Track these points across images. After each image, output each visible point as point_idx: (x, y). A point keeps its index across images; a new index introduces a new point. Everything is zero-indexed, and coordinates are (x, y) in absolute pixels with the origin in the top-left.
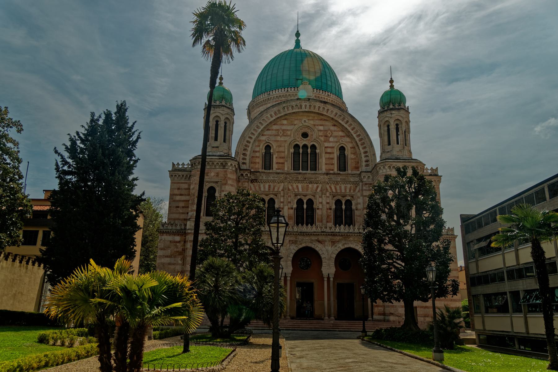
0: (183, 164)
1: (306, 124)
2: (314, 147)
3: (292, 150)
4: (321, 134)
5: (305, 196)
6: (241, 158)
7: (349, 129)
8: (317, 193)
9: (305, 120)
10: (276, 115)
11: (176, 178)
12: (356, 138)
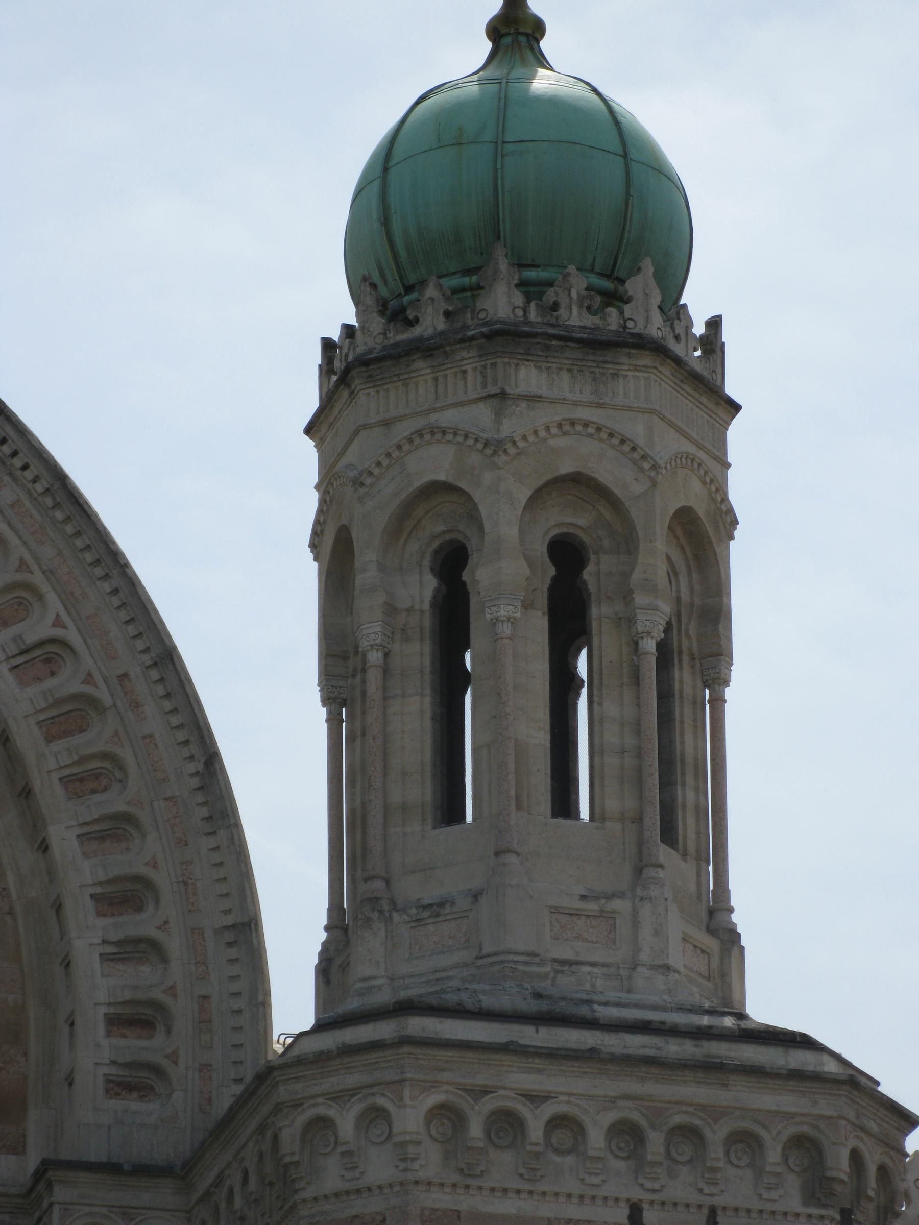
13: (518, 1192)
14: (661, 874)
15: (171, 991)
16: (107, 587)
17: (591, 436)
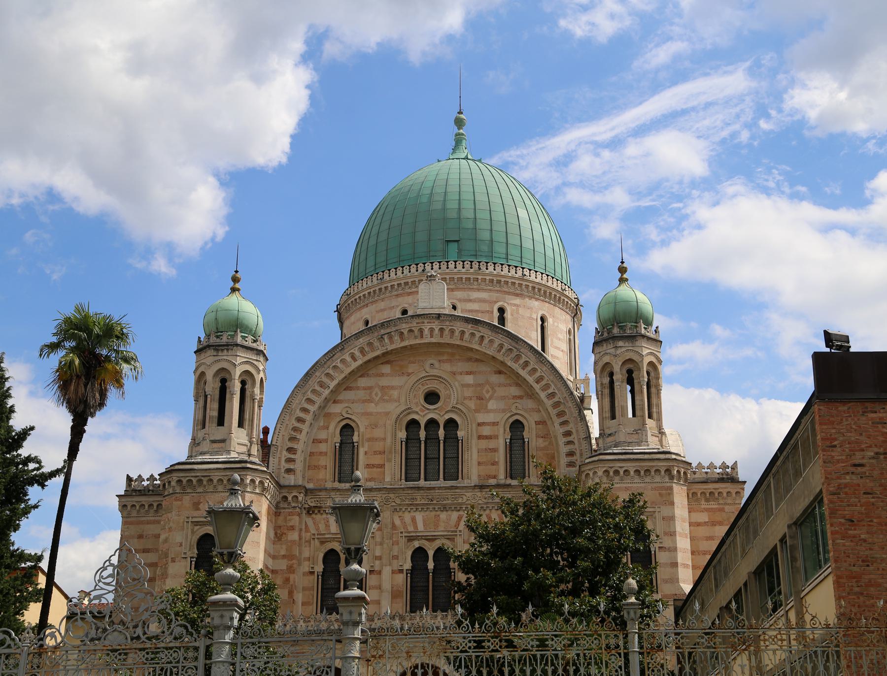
0: (152, 478)
2: (451, 424)
3: (402, 435)
4: (468, 393)
5: (431, 539)
6: (283, 459)
7: (530, 380)
8: (458, 533)
9: (432, 361)
10: (364, 355)
11: (134, 513)
12: (545, 400)
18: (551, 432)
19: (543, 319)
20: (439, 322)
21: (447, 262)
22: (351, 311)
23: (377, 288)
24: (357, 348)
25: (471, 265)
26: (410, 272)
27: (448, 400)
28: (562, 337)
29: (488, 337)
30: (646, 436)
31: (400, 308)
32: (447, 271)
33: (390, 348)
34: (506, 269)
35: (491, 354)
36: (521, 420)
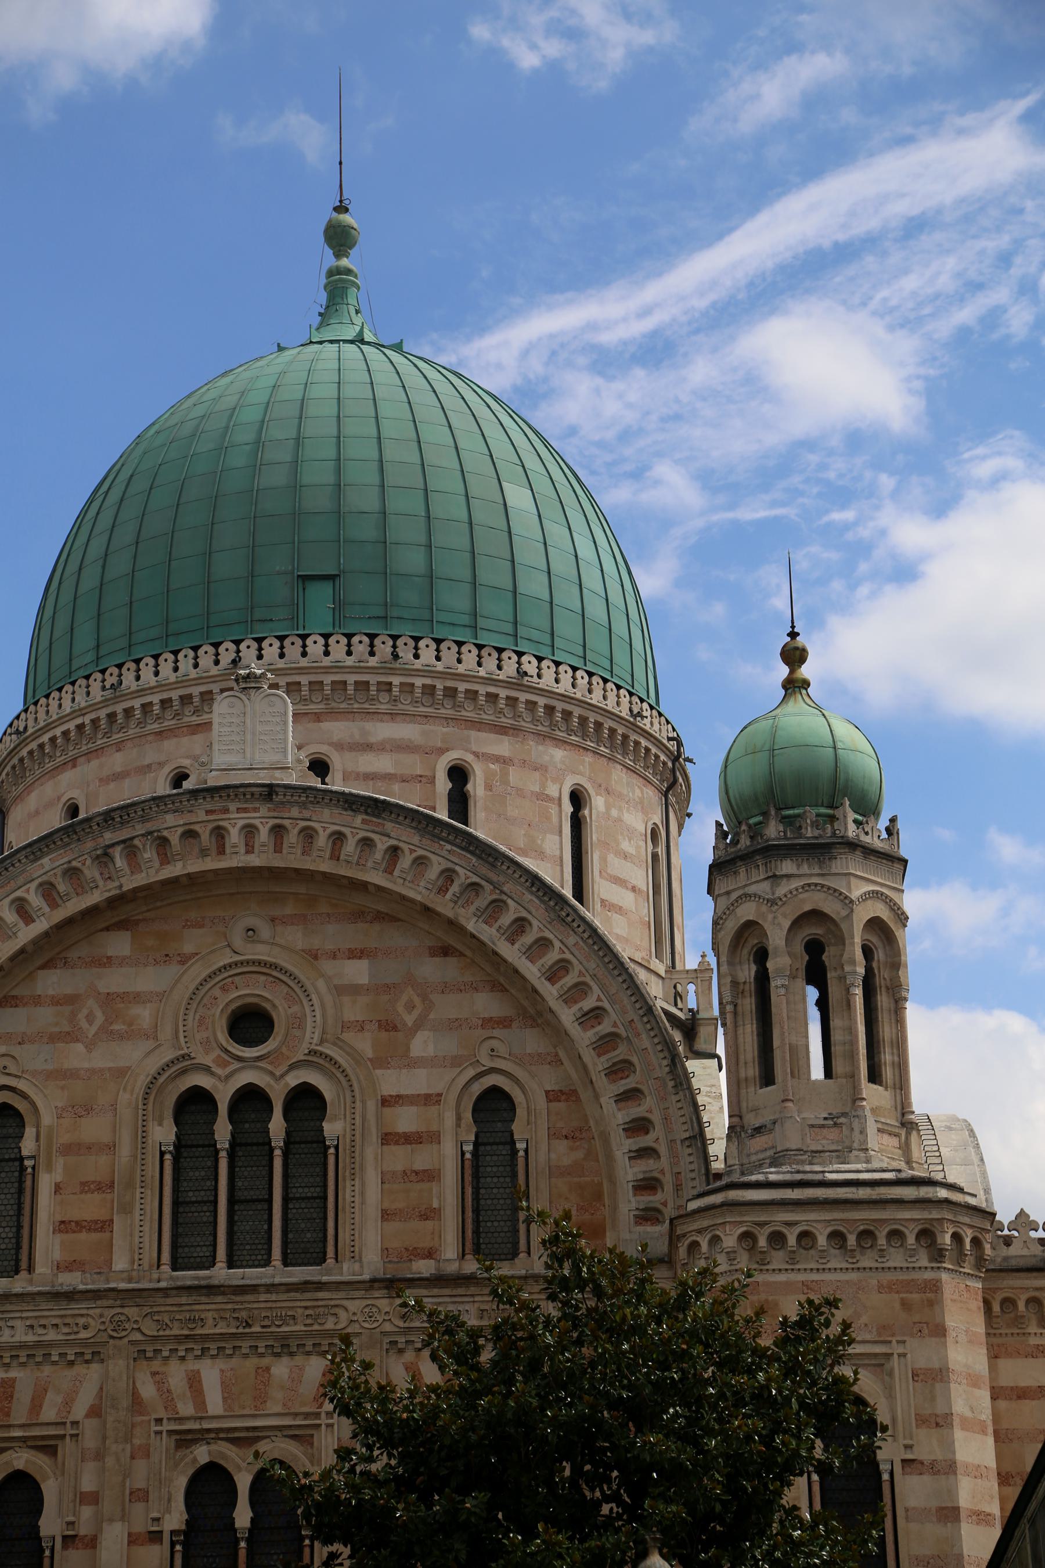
1: (260, 947)
3: (165, 1133)
4: (353, 1010)
7: (532, 971)
10: (53, 905)
13: (786, 1270)
14: (864, 1103)
15: (662, 1172)
16: (620, 979)
17: (819, 890)
18: (592, 1123)
19: (577, 798)
20: (269, 810)
21: (304, 637)
22: (29, 780)
23: (103, 714)
24: (33, 886)
25: (372, 645)
26: (196, 666)
27: (297, 1033)
28: (632, 850)
29: (412, 851)
30: (863, 1132)
31: (167, 769)
32: (304, 662)
33: (131, 882)
34: (470, 657)
35: (419, 898)
36: (507, 1089)
